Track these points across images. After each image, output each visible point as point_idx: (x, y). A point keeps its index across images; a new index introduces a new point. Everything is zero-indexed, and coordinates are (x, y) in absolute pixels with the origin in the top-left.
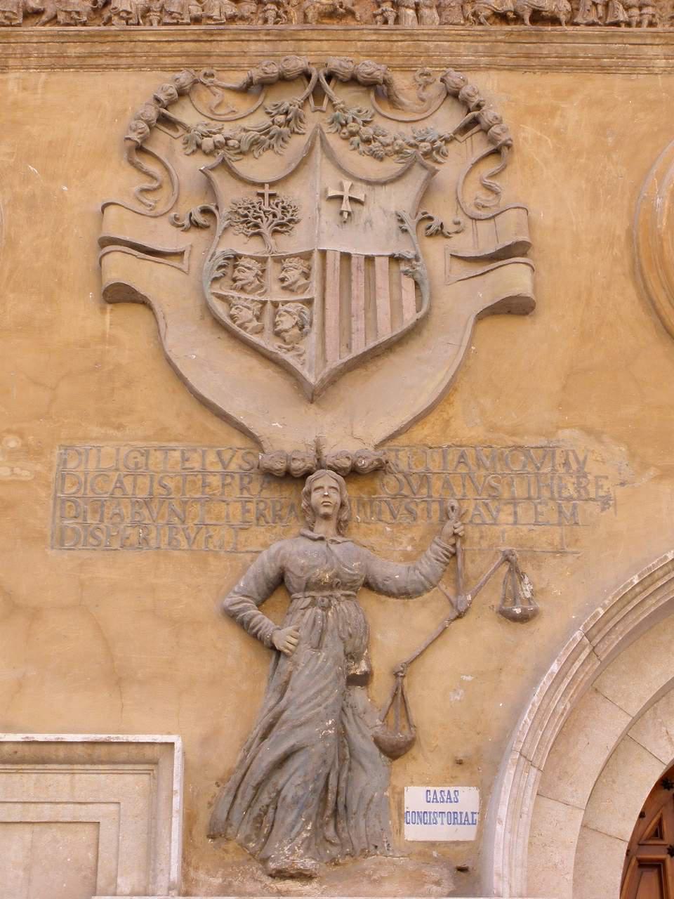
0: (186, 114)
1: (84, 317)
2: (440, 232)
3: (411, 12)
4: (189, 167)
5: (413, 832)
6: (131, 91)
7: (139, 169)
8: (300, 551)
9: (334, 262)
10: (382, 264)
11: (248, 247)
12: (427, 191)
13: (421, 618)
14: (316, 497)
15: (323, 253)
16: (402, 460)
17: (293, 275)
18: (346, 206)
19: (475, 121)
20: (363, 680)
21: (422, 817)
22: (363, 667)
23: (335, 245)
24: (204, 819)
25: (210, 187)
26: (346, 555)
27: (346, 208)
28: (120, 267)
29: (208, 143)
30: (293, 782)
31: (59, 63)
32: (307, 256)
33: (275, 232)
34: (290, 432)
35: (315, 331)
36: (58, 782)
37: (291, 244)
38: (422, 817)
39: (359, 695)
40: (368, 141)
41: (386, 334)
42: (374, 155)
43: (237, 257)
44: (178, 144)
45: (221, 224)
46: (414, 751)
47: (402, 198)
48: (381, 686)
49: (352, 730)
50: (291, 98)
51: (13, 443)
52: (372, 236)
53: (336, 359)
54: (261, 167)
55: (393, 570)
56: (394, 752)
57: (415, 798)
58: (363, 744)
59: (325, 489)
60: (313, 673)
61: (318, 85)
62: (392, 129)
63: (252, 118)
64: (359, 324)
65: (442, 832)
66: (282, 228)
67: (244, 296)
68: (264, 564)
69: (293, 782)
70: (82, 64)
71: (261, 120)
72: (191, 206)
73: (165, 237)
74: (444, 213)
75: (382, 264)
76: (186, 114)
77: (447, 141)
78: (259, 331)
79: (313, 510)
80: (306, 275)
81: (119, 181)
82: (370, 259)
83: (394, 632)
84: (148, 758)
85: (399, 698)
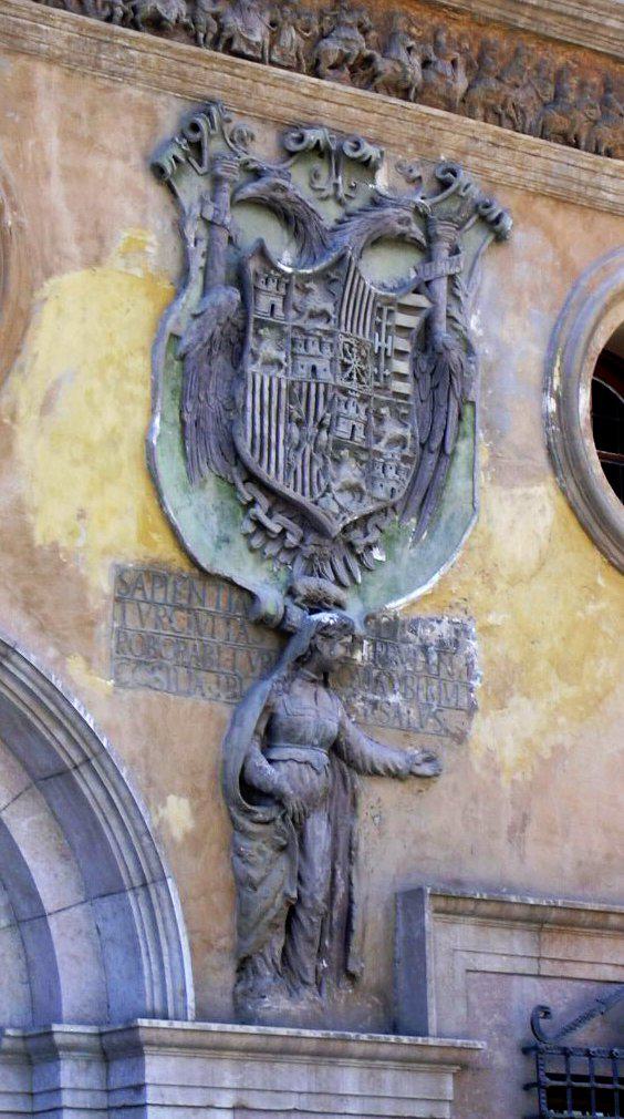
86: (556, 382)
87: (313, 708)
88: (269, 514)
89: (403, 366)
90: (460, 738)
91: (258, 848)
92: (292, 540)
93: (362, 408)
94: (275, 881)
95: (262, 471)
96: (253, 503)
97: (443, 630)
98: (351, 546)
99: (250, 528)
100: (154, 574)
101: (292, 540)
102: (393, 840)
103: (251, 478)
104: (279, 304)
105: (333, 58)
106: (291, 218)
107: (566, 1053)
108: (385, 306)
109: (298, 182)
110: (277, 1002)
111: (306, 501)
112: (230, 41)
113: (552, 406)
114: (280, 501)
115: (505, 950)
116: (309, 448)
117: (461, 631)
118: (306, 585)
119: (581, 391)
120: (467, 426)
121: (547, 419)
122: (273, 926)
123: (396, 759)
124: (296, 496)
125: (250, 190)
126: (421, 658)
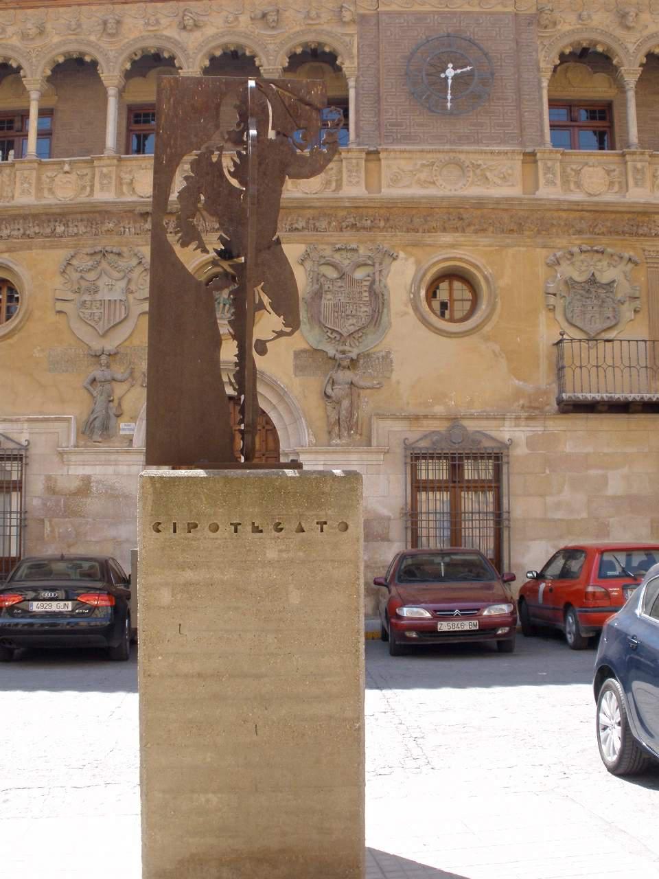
0: (74, 262)
1: (52, 318)
2: (132, 292)
3: (127, 230)
4: (75, 276)
5: (122, 433)
6: (61, 254)
7: (64, 277)
8: (98, 373)
9: (107, 303)
10: (118, 302)
11: (87, 297)
12: (129, 281)
13: (125, 386)
14: (102, 361)
15: (104, 300)
16: (121, 350)
17: (98, 305)
18: (110, 286)
19: (141, 262)
20: (112, 401)
21: (124, 429)
22: (112, 398)
23: (107, 298)
24: (80, 430)
25: (79, 283)
26: (108, 374)
27: (111, 288)
28: (59, 306)
29: (79, 269)
30: (97, 423)
31: (44, 248)
32: (101, 301)
33: (94, 293)
34: (97, 345)
35: (102, 320)
36: (51, 424)
37: (99, 297)
38: (124, 429)
39: (111, 404)
40: (116, 268)
41: (118, 321)
42: (117, 271)
43: (85, 301)
44: (72, 270)
45: (82, 292)
46: (123, 416)
47: (123, 284)
48: (116, 402)
49: (109, 412)
50: (98, 257)
51: (39, 348)
52: (116, 295)
53: (106, 328)
54: (91, 276)
55: (119, 376)
56: (118, 416)
57: (122, 425)
58: (111, 414)
59: (104, 359)
60: (101, 400)
61: (104, 254)
62: (122, 263)
63: (90, 263)
64: (112, 318)
65: (127, 433)
66: (96, 292)
67: (87, 311)
68: (91, 377)
69: (97, 423)
70: (50, 248)
71: (90, 263)
72: (76, 287)
73: (70, 296)
74: (133, 287)
75: (118, 302)
76: (74, 262)
77: (134, 267)
78: (90, 320)
79: (101, 364)
80: (101, 305)
81: (58, 281)
82: (115, 301)
83: (119, 389)
84: (68, 420)
85: (119, 404)
86: (413, 290)
87: (344, 376)
88: (332, 333)
89: (366, 294)
90: (389, 378)
91: (329, 408)
92: (338, 339)
93: (355, 306)
94: (333, 417)
95: (326, 325)
96: (327, 332)
97: (384, 353)
98: (354, 337)
99: (327, 337)
100: (304, 351)
101: (338, 339)
102: (367, 404)
103: (326, 327)
104: (331, 286)
105: (345, 226)
106: (334, 266)
107: (413, 449)
108: (360, 282)
109: (337, 257)
110: (336, 441)
111: (339, 330)
112: (317, 229)
113: (412, 296)
114: (333, 331)
115: (398, 426)
116: (340, 317)
117: (389, 353)
118: (341, 348)
119: (421, 290)
120: (385, 305)
121: (411, 299)
122: (335, 424)
123: (369, 384)
124: (337, 329)
125: (323, 261)
126: (377, 361)
